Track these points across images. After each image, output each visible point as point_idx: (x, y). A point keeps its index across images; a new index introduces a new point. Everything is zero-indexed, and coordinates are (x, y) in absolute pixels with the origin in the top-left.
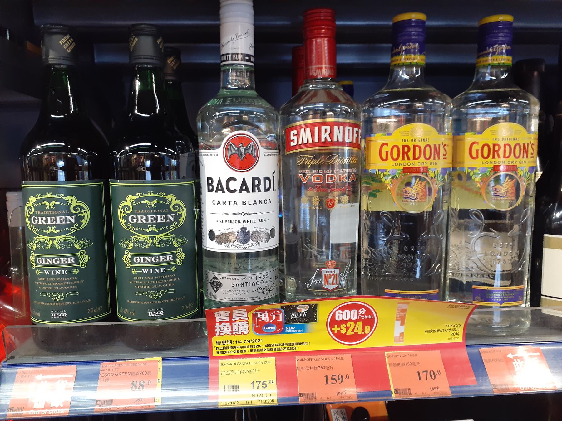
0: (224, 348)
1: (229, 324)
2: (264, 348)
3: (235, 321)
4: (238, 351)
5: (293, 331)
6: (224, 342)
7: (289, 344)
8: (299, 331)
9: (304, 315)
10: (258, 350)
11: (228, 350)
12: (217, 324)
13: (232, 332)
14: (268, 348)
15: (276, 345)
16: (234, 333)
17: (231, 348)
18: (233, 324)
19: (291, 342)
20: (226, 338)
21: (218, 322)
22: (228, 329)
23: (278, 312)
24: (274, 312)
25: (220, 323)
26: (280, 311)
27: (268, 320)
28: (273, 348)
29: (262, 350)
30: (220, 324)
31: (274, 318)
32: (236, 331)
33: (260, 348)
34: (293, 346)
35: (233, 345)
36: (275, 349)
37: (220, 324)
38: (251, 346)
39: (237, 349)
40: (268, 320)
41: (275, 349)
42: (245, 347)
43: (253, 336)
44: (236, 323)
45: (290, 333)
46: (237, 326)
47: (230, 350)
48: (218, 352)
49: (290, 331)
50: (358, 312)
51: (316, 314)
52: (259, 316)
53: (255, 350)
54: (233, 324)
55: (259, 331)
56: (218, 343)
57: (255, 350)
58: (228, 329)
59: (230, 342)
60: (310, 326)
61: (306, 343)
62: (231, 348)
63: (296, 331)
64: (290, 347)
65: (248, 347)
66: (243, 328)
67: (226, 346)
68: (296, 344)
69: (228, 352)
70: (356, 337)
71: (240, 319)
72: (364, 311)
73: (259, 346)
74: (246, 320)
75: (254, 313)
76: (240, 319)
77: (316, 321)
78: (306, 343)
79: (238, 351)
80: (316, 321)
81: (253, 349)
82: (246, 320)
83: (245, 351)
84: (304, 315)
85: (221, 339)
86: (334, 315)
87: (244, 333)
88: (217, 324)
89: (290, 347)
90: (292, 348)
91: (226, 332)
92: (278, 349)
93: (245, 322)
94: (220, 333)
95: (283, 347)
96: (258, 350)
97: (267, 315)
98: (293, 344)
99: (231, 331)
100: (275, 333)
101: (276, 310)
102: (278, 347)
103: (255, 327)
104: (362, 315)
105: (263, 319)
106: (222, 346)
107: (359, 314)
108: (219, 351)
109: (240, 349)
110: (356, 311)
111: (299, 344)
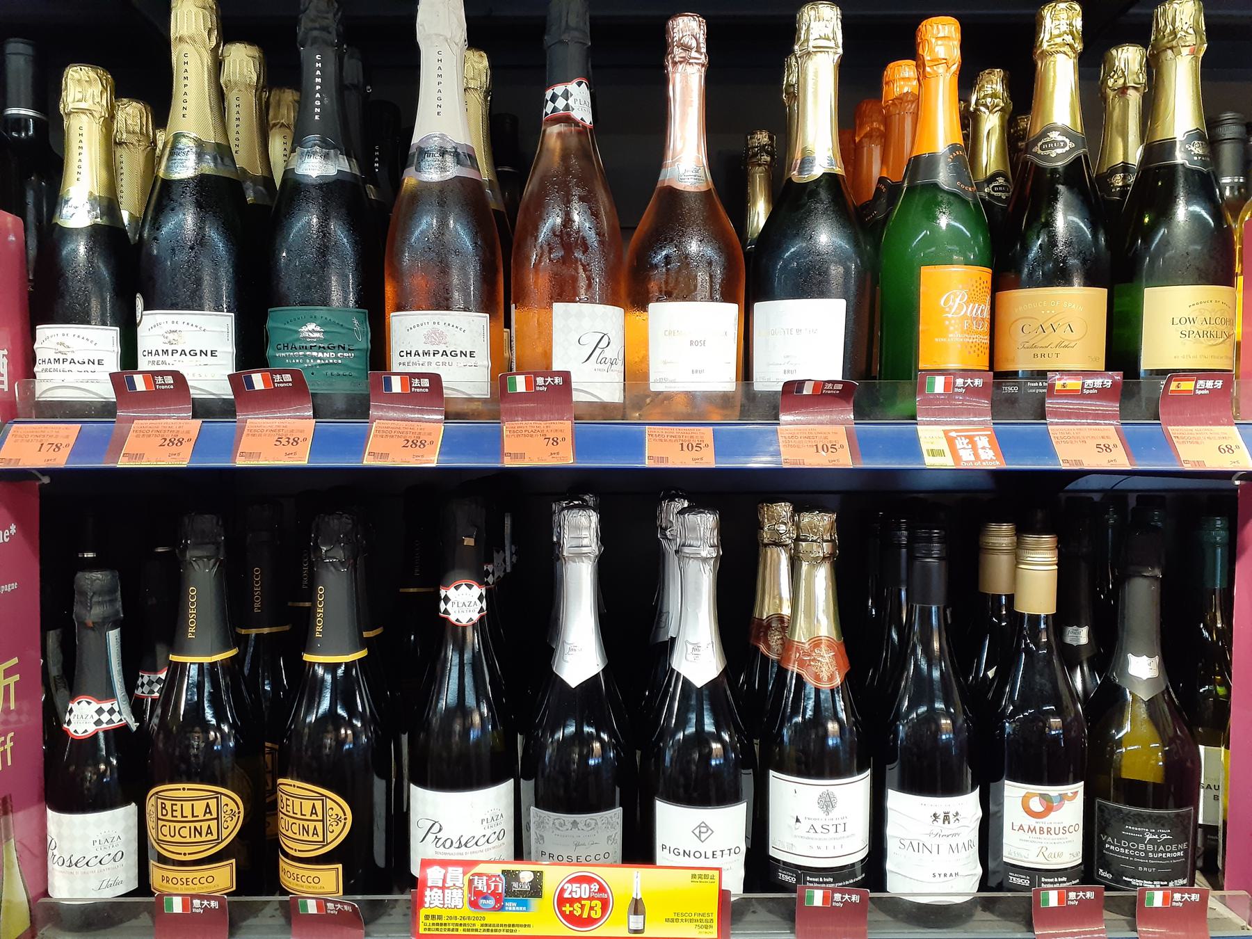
0: (433, 924)
1: (441, 891)
2: (478, 927)
3: (448, 888)
4: (449, 930)
5: (514, 909)
6: (433, 917)
7: (509, 926)
8: (521, 908)
9: (527, 888)
10: (473, 930)
11: (437, 927)
12: (428, 889)
13: (444, 904)
14: (484, 928)
15: (494, 925)
16: (446, 906)
18: (446, 891)
19: (511, 924)
20: (436, 912)
21: (429, 887)
22: (439, 898)
23: (498, 879)
24: (494, 879)
25: (431, 888)
27: (485, 891)
28: (490, 928)
29: (477, 930)
30: (431, 891)
31: (493, 888)
32: (448, 902)
33: (474, 928)
34: (514, 929)
35: (443, 922)
36: (492, 931)
38: (465, 925)
39: (447, 927)
40: (485, 891)
41: (492, 931)
42: (457, 925)
43: (468, 911)
45: (511, 911)
46: (450, 895)
47: (440, 927)
48: (425, 929)
49: (510, 909)
50: (590, 889)
51: (541, 886)
52: (476, 882)
53: (468, 930)
54: (446, 891)
55: (474, 905)
56: (427, 917)
57: (468, 930)
58: (439, 898)
59: (440, 917)
60: (534, 902)
61: (529, 926)
62: (441, 924)
63: (517, 908)
64: (509, 928)
66: (457, 899)
67: (435, 922)
68: (518, 925)
69: (437, 930)
70: (590, 921)
71: (454, 885)
72: (597, 887)
73: (474, 925)
75: (471, 878)
76: (454, 885)
78: (529, 926)
79: (449, 930)
81: (467, 928)
82: (461, 888)
83: (457, 930)
84: (527, 888)
85: (430, 912)
86: (562, 891)
87: (458, 907)
88: (428, 889)
89: (509, 928)
90: (512, 931)
91: (437, 903)
92: (496, 931)
93: (460, 891)
94: (430, 904)
95: (501, 928)
96: (473, 930)
98: (513, 925)
99: (442, 902)
100: (494, 909)
102: (496, 928)
103: (470, 899)
104: (595, 893)
105: (480, 889)
106: (431, 922)
107: (592, 890)
108: (427, 927)
109: (451, 927)
110: (587, 886)
111: (521, 926)
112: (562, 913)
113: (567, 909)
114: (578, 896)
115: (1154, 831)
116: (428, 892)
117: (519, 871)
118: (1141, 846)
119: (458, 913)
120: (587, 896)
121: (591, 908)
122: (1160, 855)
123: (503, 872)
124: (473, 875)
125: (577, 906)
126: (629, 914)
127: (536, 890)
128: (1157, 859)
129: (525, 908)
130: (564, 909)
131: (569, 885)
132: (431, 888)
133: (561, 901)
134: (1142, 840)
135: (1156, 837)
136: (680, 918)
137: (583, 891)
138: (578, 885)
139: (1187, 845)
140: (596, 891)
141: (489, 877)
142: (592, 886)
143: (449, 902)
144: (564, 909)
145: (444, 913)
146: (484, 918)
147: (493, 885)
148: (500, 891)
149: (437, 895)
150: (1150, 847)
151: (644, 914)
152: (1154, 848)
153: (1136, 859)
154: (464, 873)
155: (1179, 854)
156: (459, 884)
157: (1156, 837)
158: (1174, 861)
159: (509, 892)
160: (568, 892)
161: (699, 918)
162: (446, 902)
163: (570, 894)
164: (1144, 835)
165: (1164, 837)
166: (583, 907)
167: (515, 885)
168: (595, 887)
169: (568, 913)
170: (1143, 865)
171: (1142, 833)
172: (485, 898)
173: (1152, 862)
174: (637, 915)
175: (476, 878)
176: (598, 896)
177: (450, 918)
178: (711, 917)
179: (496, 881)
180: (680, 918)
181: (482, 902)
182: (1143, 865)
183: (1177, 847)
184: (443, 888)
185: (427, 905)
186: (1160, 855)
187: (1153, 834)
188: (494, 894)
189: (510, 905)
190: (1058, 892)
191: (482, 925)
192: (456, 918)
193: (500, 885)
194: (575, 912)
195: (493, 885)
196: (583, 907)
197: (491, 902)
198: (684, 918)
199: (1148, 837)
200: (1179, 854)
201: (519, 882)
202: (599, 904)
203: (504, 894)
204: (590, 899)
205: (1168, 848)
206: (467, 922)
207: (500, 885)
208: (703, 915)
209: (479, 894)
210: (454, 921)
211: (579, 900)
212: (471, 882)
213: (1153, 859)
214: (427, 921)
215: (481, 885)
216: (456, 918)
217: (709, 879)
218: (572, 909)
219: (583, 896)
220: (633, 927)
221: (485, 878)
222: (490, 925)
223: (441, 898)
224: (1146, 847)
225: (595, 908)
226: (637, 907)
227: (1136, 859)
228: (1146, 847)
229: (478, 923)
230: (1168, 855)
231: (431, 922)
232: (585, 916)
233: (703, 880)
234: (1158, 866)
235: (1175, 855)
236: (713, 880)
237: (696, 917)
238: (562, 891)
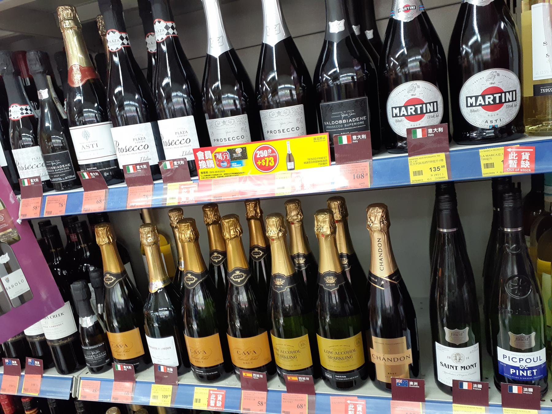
0: (205, 176)
2: (223, 175)
3: (207, 160)
5: (236, 166)
6: (204, 172)
7: (235, 173)
8: (239, 165)
9: (240, 155)
12: (199, 161)
13: (207, 167)
14: (226, 175)
15: (229, 174)
16: (208, 167)
17: (208, 175)
18: (207, 161)
20: (205, 170)
23: (226, 153)
24: (224, 154)
25: (201, 160)
26: (227, 153)
27: (222, 159)
28: (228, 175)
31: (225, 158)
33: (222, 176)
35: (209, 174)
37: (201, 161)
38: (217, 175)
39: (211, 176)
40: (222, 159)
42: (214, 175)
43: (217, 169)
44: (208, 161)
47: (207, 177)
48: (202, 178)
49: (234, 166)
50: (268, 152)
52: (217, 156)
54: (207, 161)
55: (219, 166)
56: (202, 173)
59: (207, 172)
60: (244, 161)
61: (244, 173)
62: (208, 175)
63: (237, 165)
65: (216, 175)
69: (207, 178)
70: (269, 168)
72: (271, 150)
74: (212, 159)
77: (247, 158)
78: (244, 173)
80: (247, 158)
82: (212, 159)
84: (240, 155)
85: (203, 171)
86: (256, 154)
88: (199, 161)
91: (204, 166)
93: (212, 160)
97: (221, 156)
98: (237, 173)
101: (225, 152)
103: (217, 163)
105: (219, 159)
108: (203, 177)
110: (266, 151)
112: (257, 165)
113: (259, 163)
114: (263, 156)
116: (200, 162)
117: (235, 149)
118: (340, 122)
119: (214, 170)
120: (267, 156)
121: (270, 161)
123: (228, 150)
124: (216, 153)
125: (263, 161)
126: (287, 162)
127: (244, 155)
128: (349, 127)
129: (240, 165)
130: (258, 163)
131: (258, 151)
132: (201, 160)
133: (256, 159)
134: (340, 118)
135: (347, 115)
136: (311, 161)
137: (265, 153)
138: (262, 151)
140: (270, 152)
141: (223, 153)
142: (268, 151)
143: (209, 165)
144: (258, 163)
145: (209, 170)
146: (224, 171)
147: (225, 156)
148: (228, 159)
149: (203, 163)
150: (344, 121)
151: (294, 161)
152: (346, 121)
153: (339, 130)
154: (212, 153)
156: (211, 157)
157: (347, 115)
158: (359, 127)
159: (233, 159)
160: (258, 154)
161: (320, 160)
162: (208, 166)
163: (260, 155)
164: (341, 116)
166: (266, 161)
167: (234, 155)
168: (270, 151)
169: (259, 165)
171: (340, 114)
172: (223, 162)
173: (347, 129)
174: (291, 162)
175: (217, 154)
176: (272, 155)
177: (211, 172)
178: (326, 159)
179: (225, 155)
180: (311, 161)
181: (222, 164)
184: (205, 160)
185: (201, 168)
187: (345, 114)
188: (226, 160)
189: (234, 164)
191: (224, 174)
192: (213, 172)
193: (228, 156)
194: (263, 164)
195: (225, 156)
196: (266, 161)
197: (225, 164)
198: (313, 161)
199: (343, 116)
201: (236, 153)
202: (272, 158)
203: (230, 160)
204: (268, 157)
206: (218, 173)
207: (228, 156)
208: (322, 158)
209: (220, 161)
210: (213, 174)
211: (264, 158)
212: (215, 156)
214: (202, 175)
215: (220, 157)
216: (213, 172)
217: (322, 140)
218: (261, 163)
219: (265, 156)
220: (289, 168)
221: (221, 154)
222: (228, 174)
223: (206, 164)
224: (342, 121)
225: (271, 161)
226: (290, 158)
227: (339, 130)
228: (342, 121)
229: (223, 173)
231: (204, 175)
232: (267, 165)
233: (320, 140)
236: (324, 140)
237: (319, 160)
238: (256, 154)
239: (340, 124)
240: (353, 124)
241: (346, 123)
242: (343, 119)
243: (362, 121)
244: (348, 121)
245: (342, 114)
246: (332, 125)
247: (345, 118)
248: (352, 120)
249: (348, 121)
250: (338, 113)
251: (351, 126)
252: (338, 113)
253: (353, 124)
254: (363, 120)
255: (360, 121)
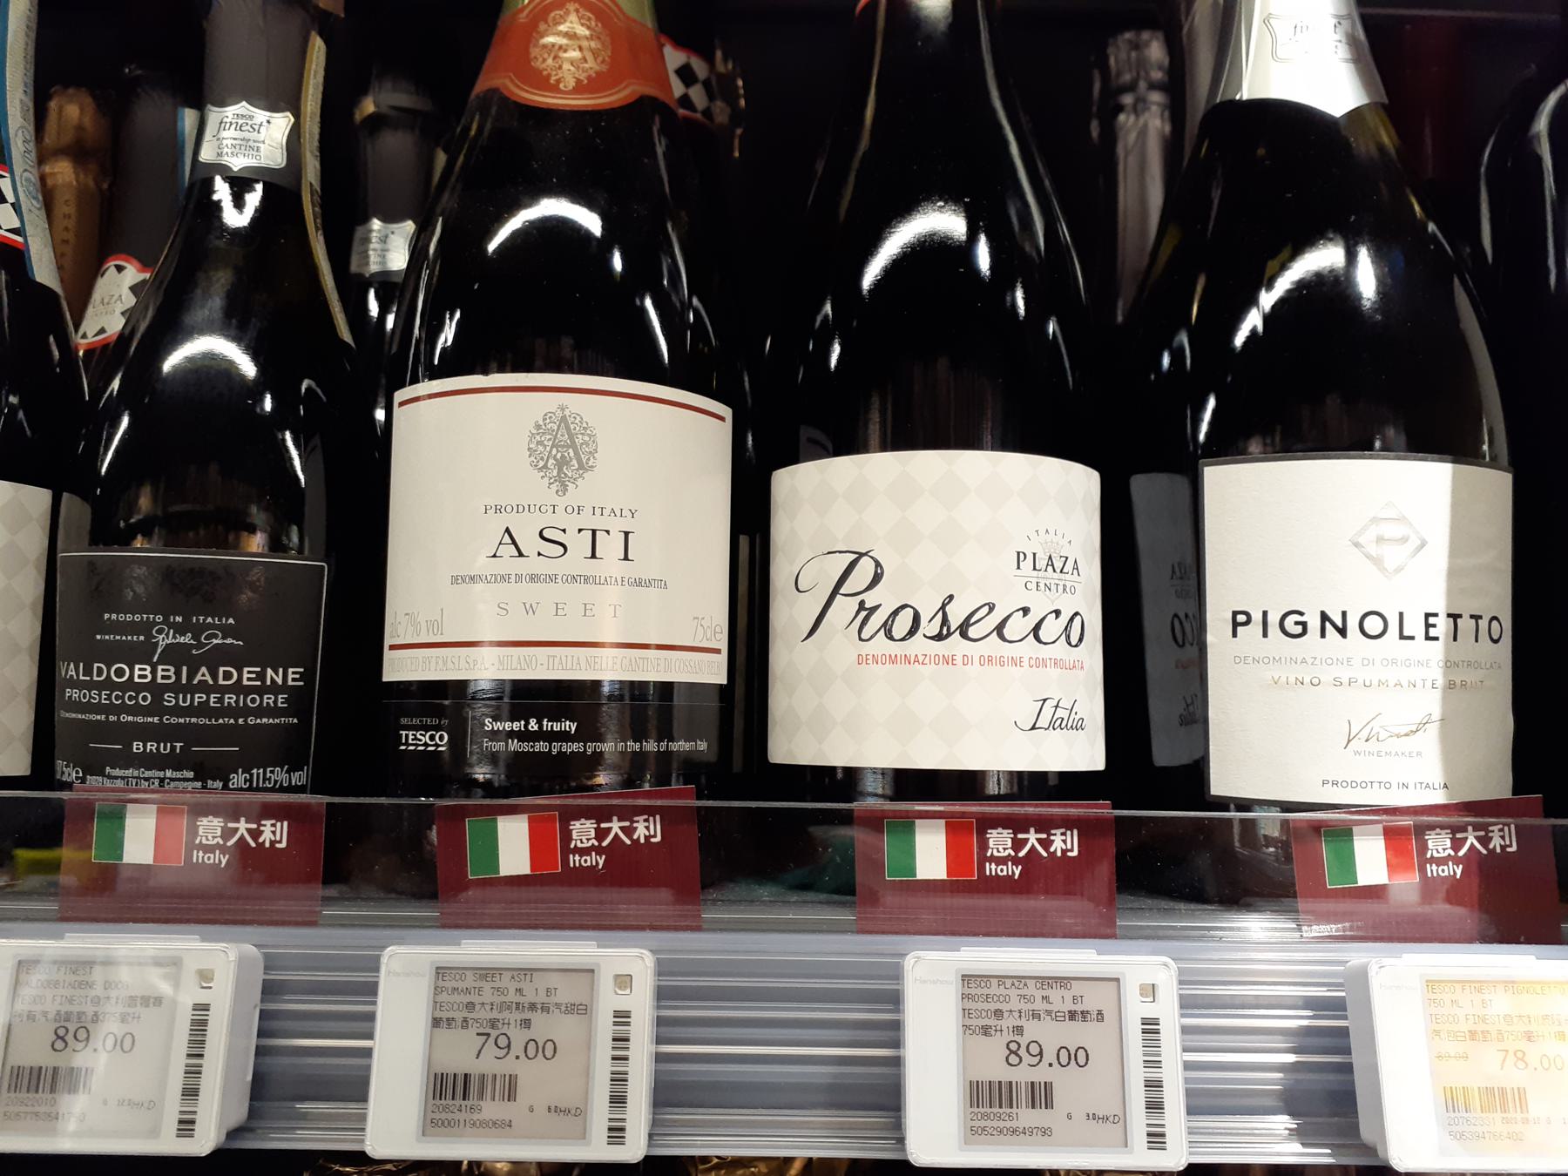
115: (179, 619)
118: (141, 672)
122: (199, 698)
134: (142, 654)
135: (186, 639)
139: (307, 677)
150: (166, 673)
152: (178, 673)
155: (268, 699)
157: (186, 639)
164: (149, 636)
165: (215, 641)
170: (145, 733)
171: (146, 628)
173: (174, 720)
182: (145, 733)
183: (261, 676)
186: (199, 698)
187: (180, 630)
190: (946, 822)
199: (163, 640)
200: (268, 699)
205: (227, 676)
213: (177, 711)
224: (154, 672)
228: (154, 672)
230: (230, 699)
234: (191, 735)
235: (253, 701)
239: (139, 688)
240: (220, 700)
241: (177, 688)
242: (161, 661)
243: (275, 689)
244: (191, 676)
245: (160, 632)
246: (91, 685)
247: (174, 655)
248: (214, 676)
249: (191, 676)
250: (137, 618)
251: (204, 709)
252: (137, 618)
253: (220, 700)
254: (284, 688)
255: (262, 691)
